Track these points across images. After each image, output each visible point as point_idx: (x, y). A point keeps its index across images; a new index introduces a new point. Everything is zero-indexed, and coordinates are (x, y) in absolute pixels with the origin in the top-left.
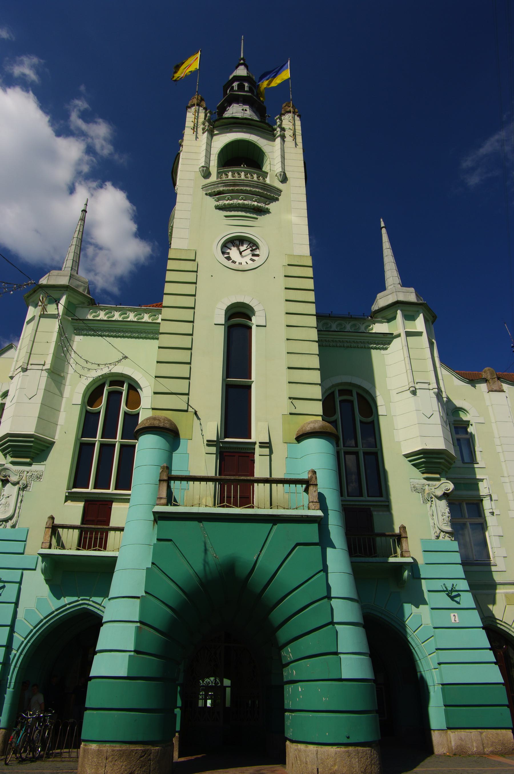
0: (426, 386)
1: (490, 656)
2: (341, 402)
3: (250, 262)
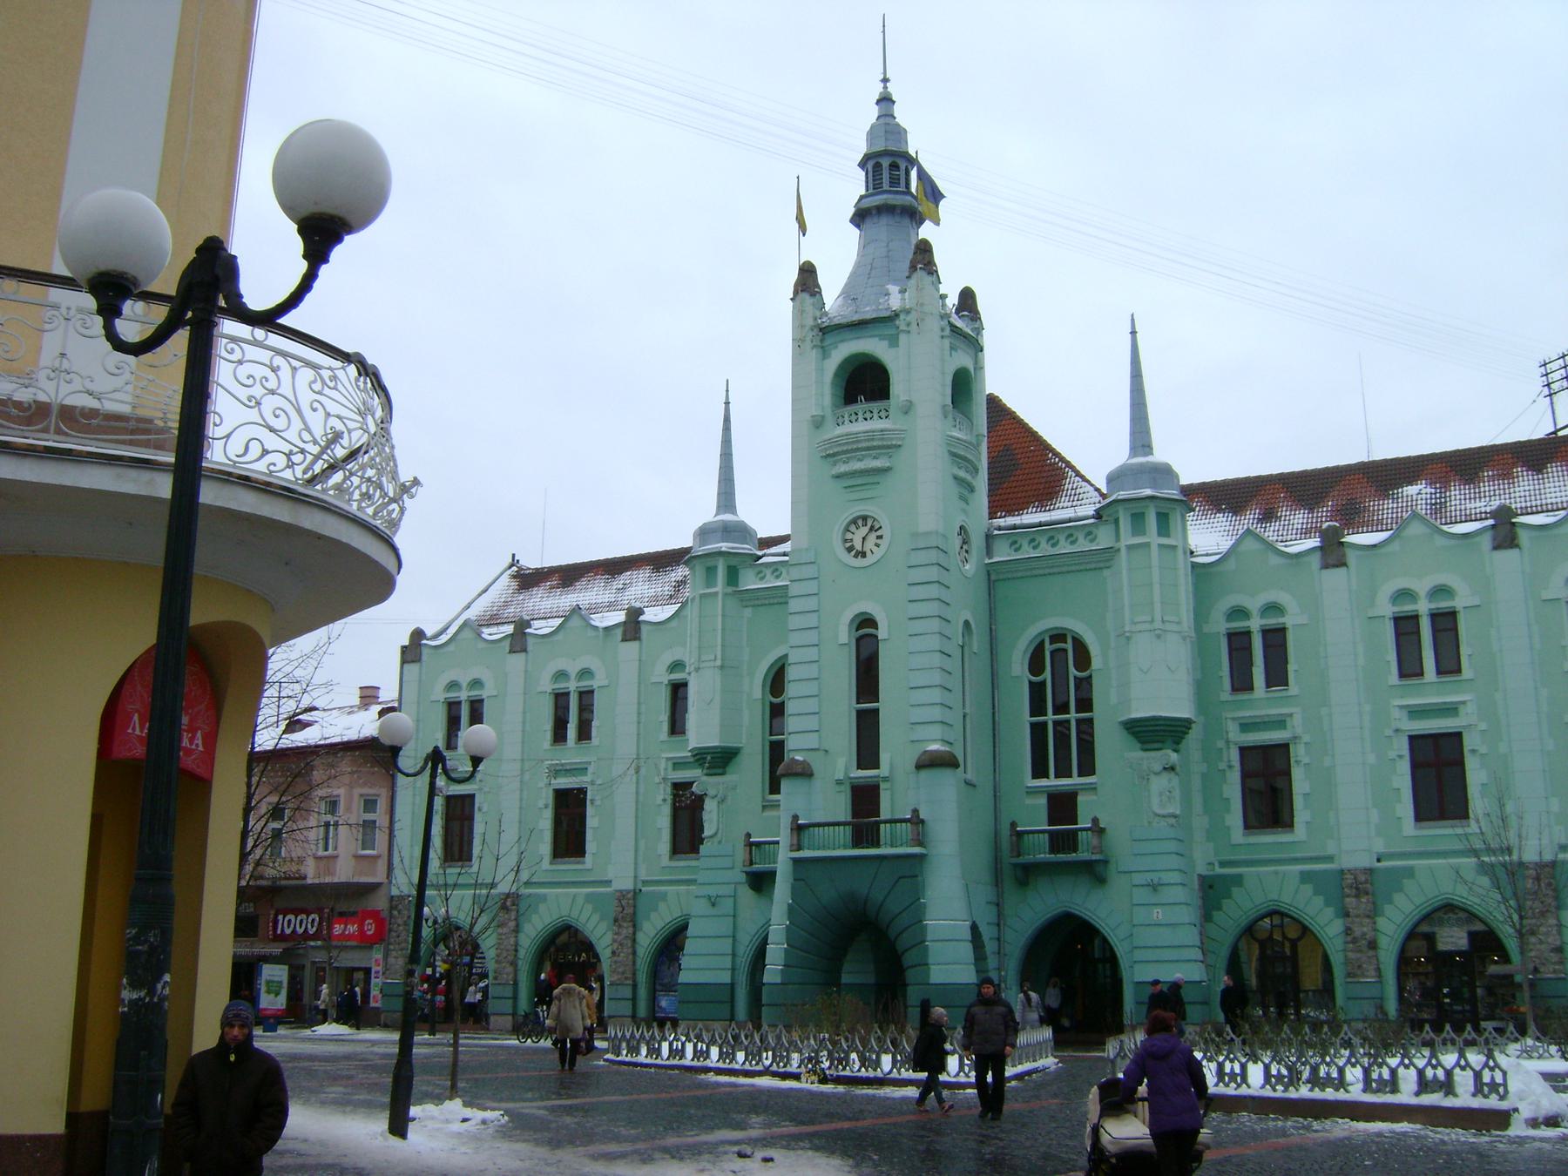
0: (1147, 626)
1: (1196, 954)
2: (1052, 653)
3: (875, 549)
